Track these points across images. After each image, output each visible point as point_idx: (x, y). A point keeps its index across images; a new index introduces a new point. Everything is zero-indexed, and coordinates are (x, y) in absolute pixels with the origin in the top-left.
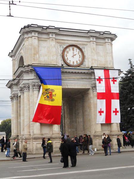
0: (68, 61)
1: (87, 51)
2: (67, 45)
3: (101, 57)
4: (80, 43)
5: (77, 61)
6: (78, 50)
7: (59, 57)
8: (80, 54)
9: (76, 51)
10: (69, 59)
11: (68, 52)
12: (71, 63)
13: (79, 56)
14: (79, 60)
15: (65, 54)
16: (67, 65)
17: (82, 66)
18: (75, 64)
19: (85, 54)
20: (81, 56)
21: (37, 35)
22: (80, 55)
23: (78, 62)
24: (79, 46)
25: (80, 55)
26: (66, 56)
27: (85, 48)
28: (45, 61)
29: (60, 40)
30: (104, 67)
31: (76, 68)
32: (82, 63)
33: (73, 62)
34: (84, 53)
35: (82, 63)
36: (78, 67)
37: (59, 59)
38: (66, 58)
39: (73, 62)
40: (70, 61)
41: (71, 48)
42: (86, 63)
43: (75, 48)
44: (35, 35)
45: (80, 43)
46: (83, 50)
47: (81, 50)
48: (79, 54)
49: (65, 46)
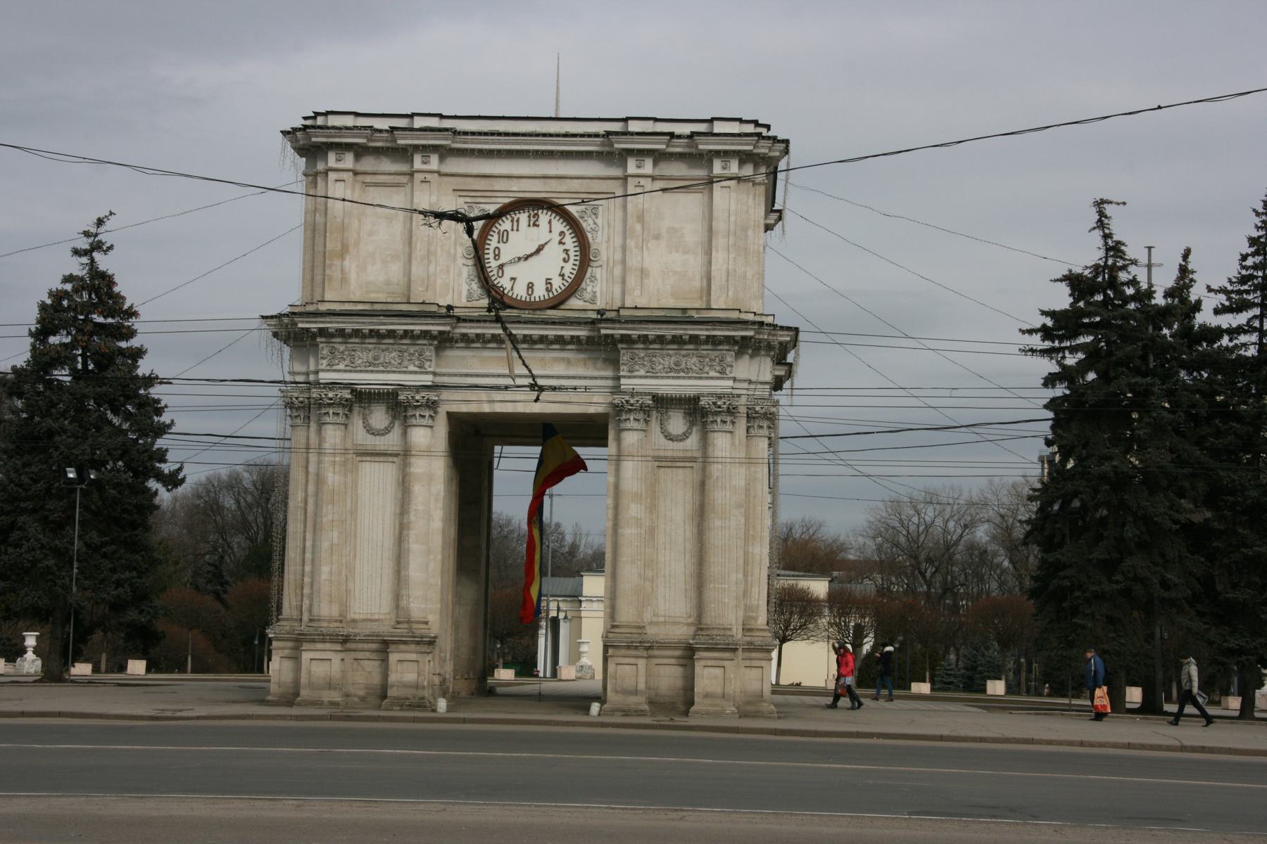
1: (609, 226)
2: (507, 201)
3: (685, 252)
4: (575, 185)
5: (548, 282)
6: (558, 225)
7: (460, 261)
8: (570, 241)
9: (549, 228)
11: (504, 237)
13: (566, 257)
14: (562, 275)
15: (492, 248)
17: (574, 303)
18: (540, 293)
19: (598, 241)
20: (572, 253)
21: (348, 161)
22: (566, 251)
23: (558, 284)
25: (566, 247)
26: (497, 256)
27: (600, 208)
28: (388, 283)
29: (470, 180)
30: (684, 310)
32: (574, 288)
33: (530, 286)
34: (589, 235)
35: (574, 288)
36: (553, 308)
37: (460, 274)
39: (530, 286)
40: (513, 279)
41: (523, 217)
42: (598, 289)
43: (544, 217)
44: (340, 165)
45: (575, 185)
46: (587, 225)
48: (561, 243)
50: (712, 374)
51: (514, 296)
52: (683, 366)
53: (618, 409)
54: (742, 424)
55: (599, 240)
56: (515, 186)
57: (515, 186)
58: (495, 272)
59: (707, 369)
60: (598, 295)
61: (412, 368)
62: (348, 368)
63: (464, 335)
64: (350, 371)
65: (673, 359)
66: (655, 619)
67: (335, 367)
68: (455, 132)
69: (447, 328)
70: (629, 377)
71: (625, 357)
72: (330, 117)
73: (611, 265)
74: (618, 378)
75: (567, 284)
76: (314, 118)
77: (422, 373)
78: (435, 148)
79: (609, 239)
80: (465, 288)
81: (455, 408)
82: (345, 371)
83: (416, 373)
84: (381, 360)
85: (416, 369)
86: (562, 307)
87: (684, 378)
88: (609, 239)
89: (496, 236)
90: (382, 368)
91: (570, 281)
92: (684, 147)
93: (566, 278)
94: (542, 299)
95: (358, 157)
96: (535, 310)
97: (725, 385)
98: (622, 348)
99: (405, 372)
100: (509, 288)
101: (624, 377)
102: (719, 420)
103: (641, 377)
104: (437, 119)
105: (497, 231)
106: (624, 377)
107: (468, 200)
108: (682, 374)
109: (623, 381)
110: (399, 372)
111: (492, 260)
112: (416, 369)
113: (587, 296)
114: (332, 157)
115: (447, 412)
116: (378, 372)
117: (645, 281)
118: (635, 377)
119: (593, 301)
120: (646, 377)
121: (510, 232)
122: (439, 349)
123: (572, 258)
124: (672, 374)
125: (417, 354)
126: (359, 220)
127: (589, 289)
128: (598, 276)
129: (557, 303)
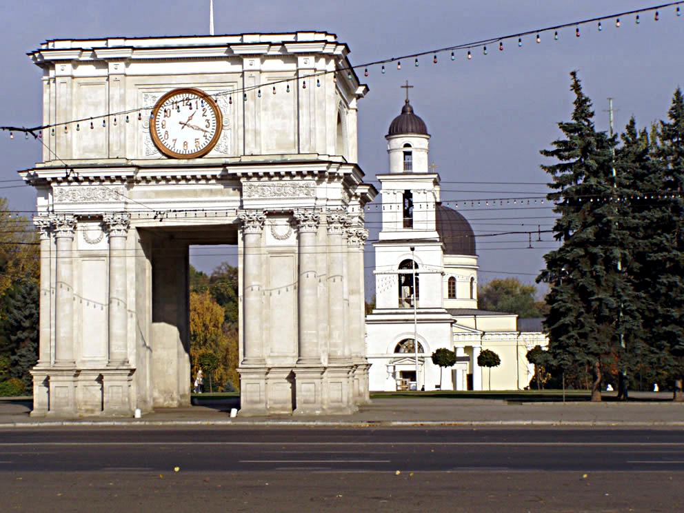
0: (169, 143)
2: (169, 90)
3: (284, 118)
10: (171, 137)
12: (179, 148)
15: (161, 121)
16: (164, 154)
17: (213, 153)
20: (211, 122)
22: (208, 121)
24: (203, 89)
26: (163, 126)
31: (191, 162)
33: (185, 144)
36: (201, 157)
37: (141, 138)
38: (162, 132)
39: (185, 144)
42: (228, 144)
46: (222, 102)
47: (213, 104)
49: (160, 95)
51: (175, 151)
52: (283, 191)
55: (228, 112)
56: (174, 80)
57: (174, 80)
58: (163, 136)
59: (298, 192)
60: (229, 147)
63: (144, 178)
64: (73, 204)
66: (272, 354)
67: (63, 202)
68: (133, 48)
69: (132, 174)
70: (249, 200)
72: (56, 43)
73: (236, 127)
75: (209, 142)
76: (47, 44)
77: (117, 203)
78: (122, 59)
79: (234, 111)
80: (144, 147)
82: (69, 204)
83: (114, 203)
86: (206, 156)
87: (283, 199)
88: (234, 111)
89: (163, 113)
90: (92, 201)
91: (210, 139)
92: (279, 51)
93: (208, 138)
94: (193, 152)
95: (75, 67)
96: (189, 159)
99: (107, 203)
100: (172, 146)
101: (246, 200)
103: (256, 199)
104: (123, 40)
105: (163, 110)
106: (246, 200)
107: (145, 90)
108: (282, 197)
110: (104, 203)
111: (161, 128)
113: (222, 149)
114: (58, 66)
116: (90, 203)
117: (258, 138)
118: (252, 200)
119: (225, 152)
120: (259, 199)
121: (172, 110)
122: (128, 187)
123: (211, 125)
124: (276, 197)
126: (77, 107)
127: (223, 144)
128: (229, 135)
129: (202, 154)
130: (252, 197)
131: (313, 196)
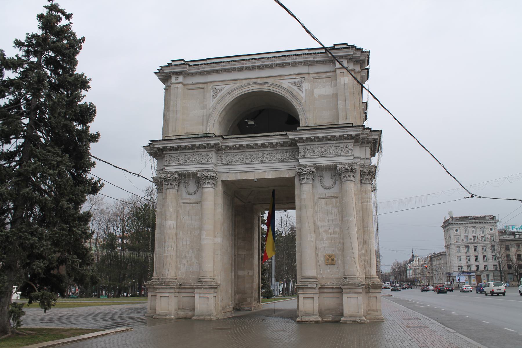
50: (342, 154)
53: (299, 174)
54: (358, 177)
61: (204, 162)
62: (177, 164)
65: (323, 149)
71: (301, 149)
74: (297, 160)
81: (224, 179)
84: (191, 159)
85: (206, 162)
97: (349, 159)
98: (300, 145)
101: (301, 158)
102: (347, 176)
109: (300, 161)
112: (206, 162)
115: (222, 181)
124: (323, 156)
125: (206, 156)
130: (306, 156)
131: (351, 154)
